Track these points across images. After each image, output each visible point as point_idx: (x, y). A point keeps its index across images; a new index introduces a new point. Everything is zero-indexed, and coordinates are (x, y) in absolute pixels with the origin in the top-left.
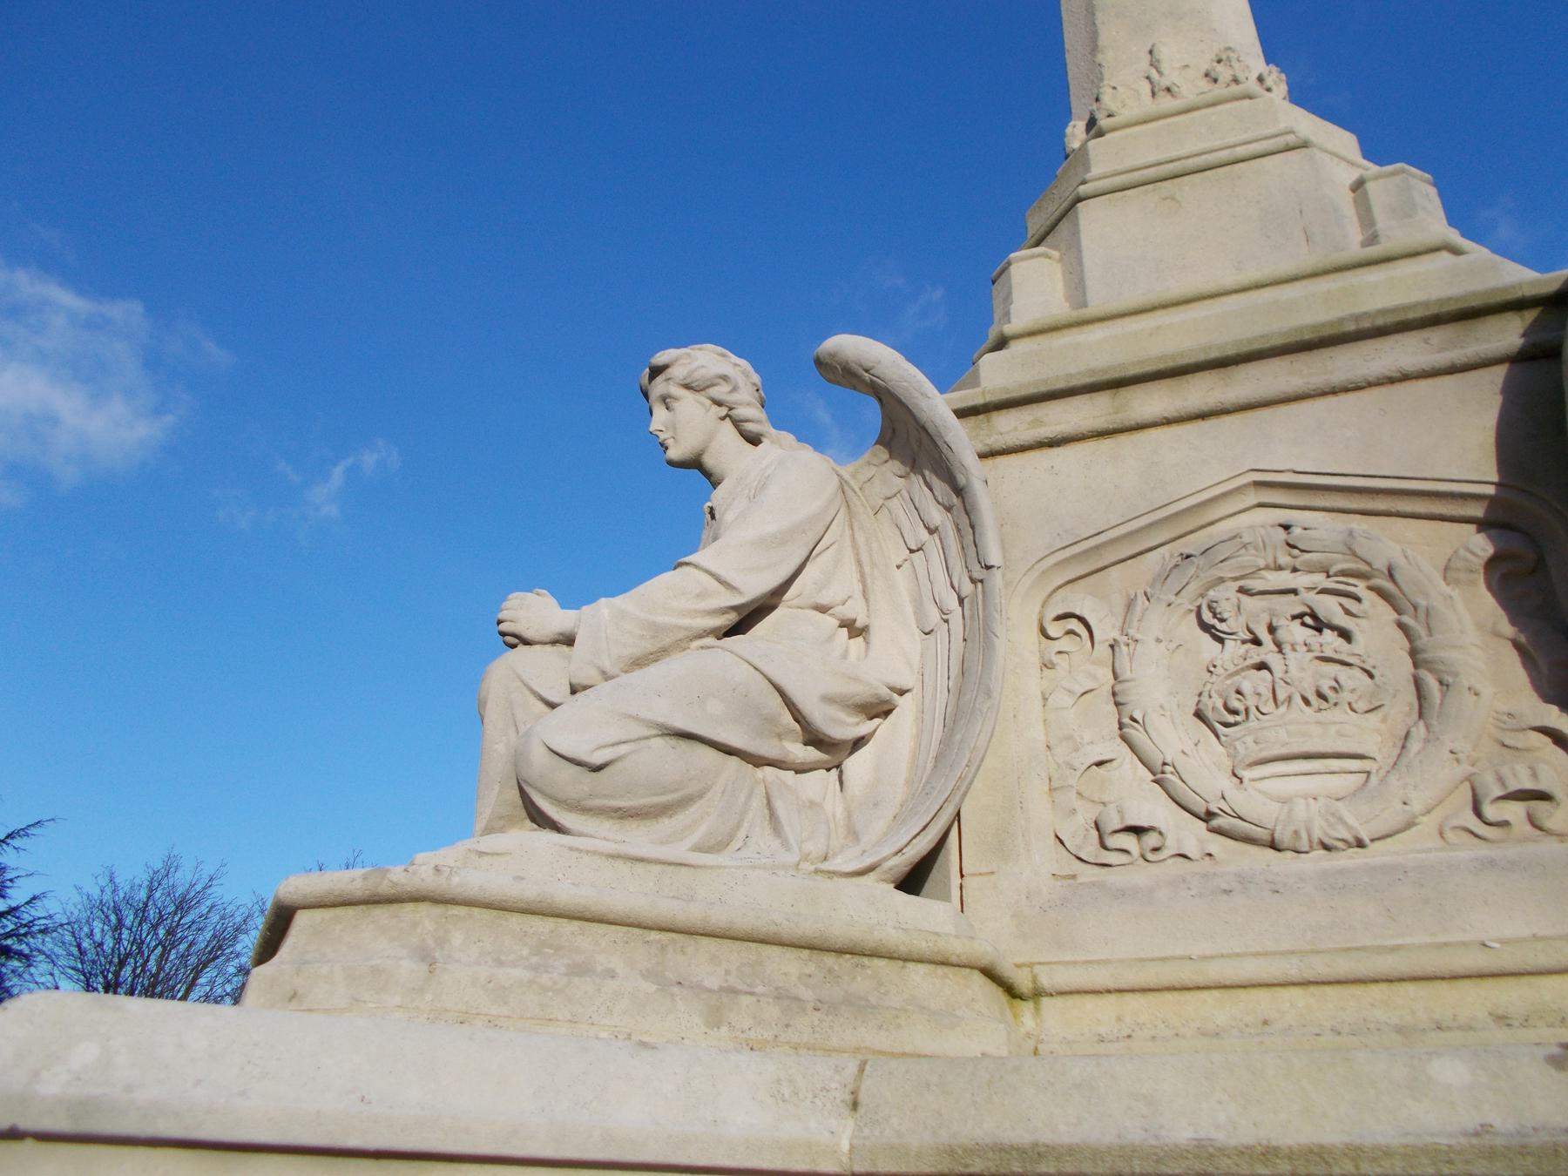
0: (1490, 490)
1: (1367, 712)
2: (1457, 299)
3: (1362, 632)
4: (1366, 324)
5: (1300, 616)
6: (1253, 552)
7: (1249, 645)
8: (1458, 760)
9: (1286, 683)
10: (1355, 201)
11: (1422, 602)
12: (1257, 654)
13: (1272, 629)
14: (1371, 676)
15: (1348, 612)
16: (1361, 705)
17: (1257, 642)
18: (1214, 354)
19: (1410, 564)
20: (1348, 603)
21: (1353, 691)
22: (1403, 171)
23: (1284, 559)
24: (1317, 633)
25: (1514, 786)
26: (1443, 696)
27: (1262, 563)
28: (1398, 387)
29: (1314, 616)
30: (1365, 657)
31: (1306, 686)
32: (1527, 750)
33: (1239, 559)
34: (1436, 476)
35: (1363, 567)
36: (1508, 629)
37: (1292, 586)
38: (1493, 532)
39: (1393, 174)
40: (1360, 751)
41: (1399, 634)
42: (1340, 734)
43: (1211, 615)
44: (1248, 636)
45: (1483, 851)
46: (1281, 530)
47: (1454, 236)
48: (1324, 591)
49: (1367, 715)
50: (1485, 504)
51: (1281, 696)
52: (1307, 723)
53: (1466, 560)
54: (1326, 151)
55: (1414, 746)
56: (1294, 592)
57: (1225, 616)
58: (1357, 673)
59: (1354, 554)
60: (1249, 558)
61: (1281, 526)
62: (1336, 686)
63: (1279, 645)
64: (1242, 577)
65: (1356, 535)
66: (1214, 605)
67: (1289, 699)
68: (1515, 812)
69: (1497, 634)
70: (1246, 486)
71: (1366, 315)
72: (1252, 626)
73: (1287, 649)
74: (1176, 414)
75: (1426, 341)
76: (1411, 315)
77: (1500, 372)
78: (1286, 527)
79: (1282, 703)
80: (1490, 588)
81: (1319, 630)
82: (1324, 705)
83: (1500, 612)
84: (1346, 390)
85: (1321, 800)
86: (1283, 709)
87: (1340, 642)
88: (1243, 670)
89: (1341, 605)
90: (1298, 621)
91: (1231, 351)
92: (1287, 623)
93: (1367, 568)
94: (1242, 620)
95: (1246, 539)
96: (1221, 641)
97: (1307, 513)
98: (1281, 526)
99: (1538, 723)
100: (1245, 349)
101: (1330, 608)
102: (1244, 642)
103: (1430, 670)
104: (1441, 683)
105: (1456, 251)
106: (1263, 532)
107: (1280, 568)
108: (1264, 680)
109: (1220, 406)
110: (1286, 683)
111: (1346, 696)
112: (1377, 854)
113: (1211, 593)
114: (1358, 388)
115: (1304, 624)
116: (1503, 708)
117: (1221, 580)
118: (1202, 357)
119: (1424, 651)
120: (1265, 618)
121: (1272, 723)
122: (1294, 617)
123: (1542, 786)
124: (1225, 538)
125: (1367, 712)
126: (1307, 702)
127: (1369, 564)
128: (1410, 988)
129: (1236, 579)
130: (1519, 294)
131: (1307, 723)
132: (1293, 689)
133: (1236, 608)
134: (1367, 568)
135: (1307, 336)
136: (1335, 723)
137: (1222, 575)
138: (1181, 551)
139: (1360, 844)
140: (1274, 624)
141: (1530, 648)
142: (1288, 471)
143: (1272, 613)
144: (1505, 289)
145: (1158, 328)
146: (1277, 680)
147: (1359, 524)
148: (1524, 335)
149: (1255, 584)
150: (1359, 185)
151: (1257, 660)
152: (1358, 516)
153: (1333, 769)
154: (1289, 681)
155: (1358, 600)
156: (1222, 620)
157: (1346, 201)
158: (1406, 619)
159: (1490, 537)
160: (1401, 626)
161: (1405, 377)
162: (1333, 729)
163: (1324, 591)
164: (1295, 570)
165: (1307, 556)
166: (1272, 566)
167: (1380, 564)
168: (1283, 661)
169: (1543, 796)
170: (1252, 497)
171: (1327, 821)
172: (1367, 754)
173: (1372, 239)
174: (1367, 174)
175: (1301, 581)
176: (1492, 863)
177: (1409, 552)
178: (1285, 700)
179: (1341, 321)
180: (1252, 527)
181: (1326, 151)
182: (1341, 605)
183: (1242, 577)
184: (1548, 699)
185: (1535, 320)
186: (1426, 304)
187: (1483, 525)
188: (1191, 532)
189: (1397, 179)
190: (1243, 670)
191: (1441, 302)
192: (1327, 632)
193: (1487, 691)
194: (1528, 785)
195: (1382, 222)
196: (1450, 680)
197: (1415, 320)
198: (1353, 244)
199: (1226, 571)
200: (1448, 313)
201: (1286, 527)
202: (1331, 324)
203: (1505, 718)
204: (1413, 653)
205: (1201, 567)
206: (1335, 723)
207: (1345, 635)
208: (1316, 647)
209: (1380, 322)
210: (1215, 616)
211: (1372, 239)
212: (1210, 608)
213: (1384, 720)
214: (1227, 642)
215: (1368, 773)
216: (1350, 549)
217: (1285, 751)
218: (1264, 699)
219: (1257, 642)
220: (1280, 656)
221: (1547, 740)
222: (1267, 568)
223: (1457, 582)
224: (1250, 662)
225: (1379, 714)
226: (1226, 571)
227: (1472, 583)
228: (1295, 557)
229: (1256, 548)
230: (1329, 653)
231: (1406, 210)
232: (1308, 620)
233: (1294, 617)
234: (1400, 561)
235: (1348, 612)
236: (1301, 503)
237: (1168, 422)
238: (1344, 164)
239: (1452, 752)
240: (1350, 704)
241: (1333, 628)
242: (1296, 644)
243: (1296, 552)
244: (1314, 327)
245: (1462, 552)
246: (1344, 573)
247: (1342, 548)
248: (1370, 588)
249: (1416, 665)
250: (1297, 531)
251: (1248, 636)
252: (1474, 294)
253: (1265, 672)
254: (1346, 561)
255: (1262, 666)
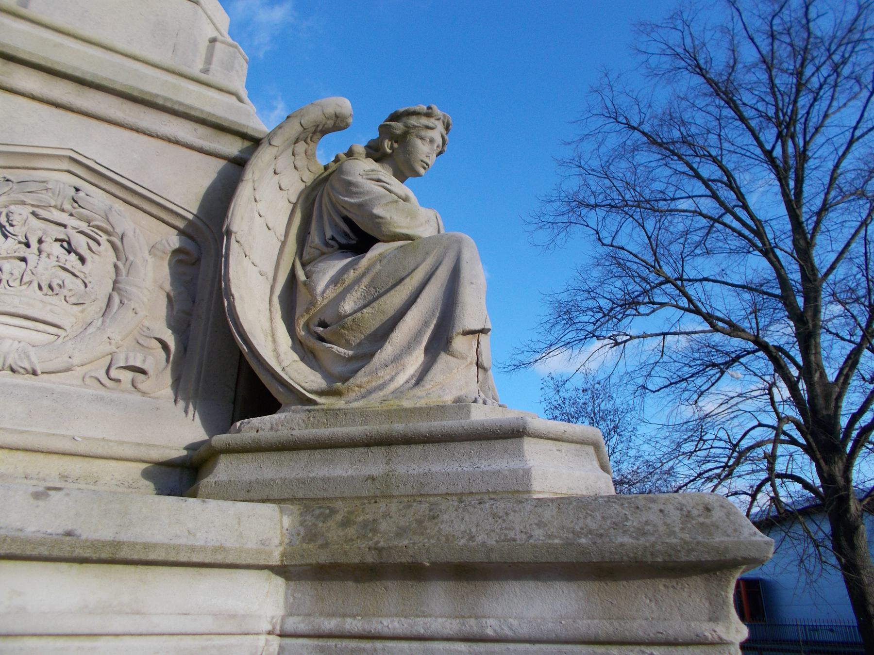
0: (190, 217)
1: (74, 304)
2: (217, 117)
3: (93, 262)
4: (169, 105)
5: (62, 241)
6: (50, 194)
7: (23, 246)
8: (110, 343)
9: (32, 273)
10: (208, 47)
11: (131, 258)
12: (23, 251)
13: (40, 241)
14: (86, 286)
15: (90, 249)
16: (73, 300)
17: (28, 245)
18: (78, 74)
19: (135, 237)
20: (93, 244)
21: (71, 290)
22: (236, 47)
23: (67, 206)
24: (67, 253)
25: (131, 363)
26: (119, 308)
27: (53, 203)
28: (172, 146)
29: (69, 243)
30: (87, 275)
31: (44, 279)
32: (148, 348)
33: (40, 195)
34: (168, 198)
35: (109, 228)
36: (168, 287)
37: (65, 223)
38: (183, 238)
39: (231, 45)
40: (59, 323)
41: (113, 269)
42: (51, 311)
43: (6, 219)
44: (24, 240)
45: (102, 392)
46: (74, 190)
47: (244, 94)
48: (81, 232)
49: (74, 306)
50: (186, 222)
51: (26, 279)
52: (34, 299)
53: (164, 246)
54: (206, 13)
55: (91, 330)
56: (65, 226)
57: (14, 223)
58: (79, 282)
59: (108, 220)
60: (46, 197)
61: (75, 188)
62: (62, 284)
63: (40, 251)
64: (38, 206)
65: (113, 209)
66: (10, 214)
67: (30, 283)
68: (126, 376)
69: (162, 288)
70: (64, 156)
71: (171, 100)
72: (28, 235)
73: (44, 255)
74: (40, 96)
75: (195, 130)
76: (193, 113)
77: (221, 163)
78: (77, 190)
79: (25, 284)
80: (170, 264)
81: (69, 252)
82: (50, 292)
83: (169, 278)
84: (144, 133)
85: (22, 344)
86: (24, 287)
87: (79, 263)
88: (11, 257)
89: (88, 243)
90: (59, 243)
91: (89, 78)
92: (51, 241)
93: (112, 230)
94: (24, 229)
95: (49, 186)
96: (6, 237)
97: (94, 188)
98: (75, 188)
99: (158, 336)
100: (97, 81)
101: (80, 243)
102: (20, 242)
103: (119, 294)
104: (121, 302)
105: (240, 100)
106: (62, 186)
107: (63, 210)
108: (20, 267)
109: (69, 105)
110: (32, 273)
111: (65, 292)
112: (41, 381)
113: (12, 208)
114: (150, 135)
115: (62, 246)
116: (147, 323)
117: (23, 203)
118: (70, 71)
119: (120, 283)
120: (40, 234)
121: (13, 293)
122: (57, 240)
123: (145, 367)
124: (37, 179)
125: (74, 304)
126: (40, 288)
127: (113, 228)
128: (21, 455)
129: (33, 206)
130: (245, 130)
131: (34, 299)
132: (34, 278)
133: (24, 221)
134: (112, 230)
135: (135, 94)
136: (51, 304)
137: (25, 200)
138: (5, 175)
139: (34, 373)
140: (43, 239)
141: (173, 299)
142: (92, 160)
143: (45, 232)
144: (240, 125)
145: (61, 44)
146: (28, 270)
147: (119, 205)
148: (240, 151)
149: (42, 213)
150: (213, 41)
151: (22, 255)
152: (121, 202)
153: (38, 329)
154: (34, 272)
155: (99, 244)
156: (12, 225)
157: (203, 45)
158: (120, 264)
159: (180, 240)
160: (116, 266)
161: (177, 143)
162: (49, 307)
163: (81, 232)
164: (71, 215)
165: (81, 210)
166: (59, 207)
167: (119, 230)
168: (37, 261)
169: (143, 372)
170: (66, 165)
171: (19, 356)
172: (62, 326)
173: (206, 71)
174: (219, 37)
175: (72, 222)
176: (102, 399)
177: (137, 231)
178: (27, 283)
179: (157, 96)
180: (57, 181)
181: (206, 13)
182: (88, 243)
183: (38, 206)
184: (170, 326)
185: (248, 147)
186: (202, 111)
187: (181, 232)
188: (19, 168)
189: (231, 49)
190: (11, 257)
191: (209, 114)
192: (73, 254)
193: (142, 313)
194: (138, 364)
195: (215, 66)
196: (126, 301)
197: (194, 116)
198: (196, 70)
199: (28, 199)
200: (211, 122)
201: (77, 190)
202: (151, 94)
203: (145, 329)
204: (115, 282)
205: (14, 189)
206: (51, 304)
207: (82, 260)
208: (62, 260)
209: (176, 107)
210: (8, 221)
211: (206, 71)
212: (7, 215)
213: (82, 311)
214: (9, 238)
215: (59, 336)
216: (106, 216)
217: (13, 310)
218: (14, 277)
219: (28, 245)
220: (38, 258)
221: (160, 346)
222: (55, 207)
223: (155, 255)
224: (17, 254)
225: (80, 308)
226: (28, 199)
227: (162, 258)
228: (74, 208)
229: (53, 193)
230: (68, 266)
231: (228, 67)
232: (65, 244)
233: (57, 240)
234: (130, 234)
235: (90, 249)
236: (93, 181)
237: (33, 98)
238: (212, 26)
239: (109, 338)
240: (65, 296)
241: (77, 254)
242: (52, 255)
243: (76, 205)
244: (142, 91)
245: (164, 241)
246: (98, 227)
247: (102, 213)
248: (109, 241)
249: (113, 289)
250: (81, 194)
251: (24, 240)
252: (226, 120)
253: (23, 263)
254: (101, 221)
255: (24, 260)
